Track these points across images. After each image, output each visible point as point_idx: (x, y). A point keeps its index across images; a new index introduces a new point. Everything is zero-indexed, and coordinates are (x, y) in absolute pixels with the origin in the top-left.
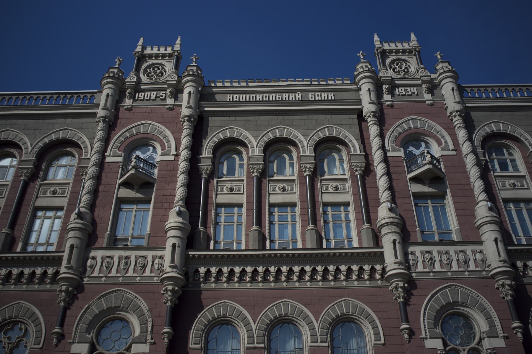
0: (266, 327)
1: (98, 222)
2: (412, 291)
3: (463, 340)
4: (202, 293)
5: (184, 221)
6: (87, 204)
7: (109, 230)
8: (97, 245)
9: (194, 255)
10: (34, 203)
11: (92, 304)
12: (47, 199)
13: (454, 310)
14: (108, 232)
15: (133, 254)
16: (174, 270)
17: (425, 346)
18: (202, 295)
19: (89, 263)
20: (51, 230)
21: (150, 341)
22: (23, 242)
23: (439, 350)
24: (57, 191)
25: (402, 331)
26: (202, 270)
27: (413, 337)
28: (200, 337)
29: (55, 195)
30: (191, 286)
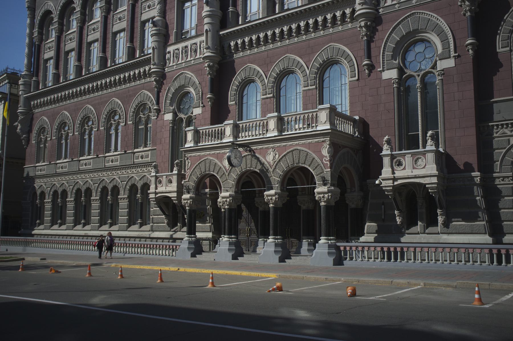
0: (274, 80)
1: (169, 24)
2: (377, 27)
3: (429, 64)
4: (234, 62)
5: (212, 9)
6: (159, 13)
7: (175, 29)
8: (170, 42)
9: (223, 34)
10: (141, 19)
11: (170, 86)
12: (147, 13)
13: (415, 38)
14: (175, 31)
15: (188, 43)
16: (208, 50)
17: (382, 78)
18: (235, 63)
19: (168, 56)
20: (200, 19)
21: (201, 105)
22: (140, 50)
23: (393, 79)
24: (151, 5)
25: (467, 47)
26: (232, 44)
27: (373, 71)
28: (234, 96)
29: (150, 9)
30: (228, 58)
